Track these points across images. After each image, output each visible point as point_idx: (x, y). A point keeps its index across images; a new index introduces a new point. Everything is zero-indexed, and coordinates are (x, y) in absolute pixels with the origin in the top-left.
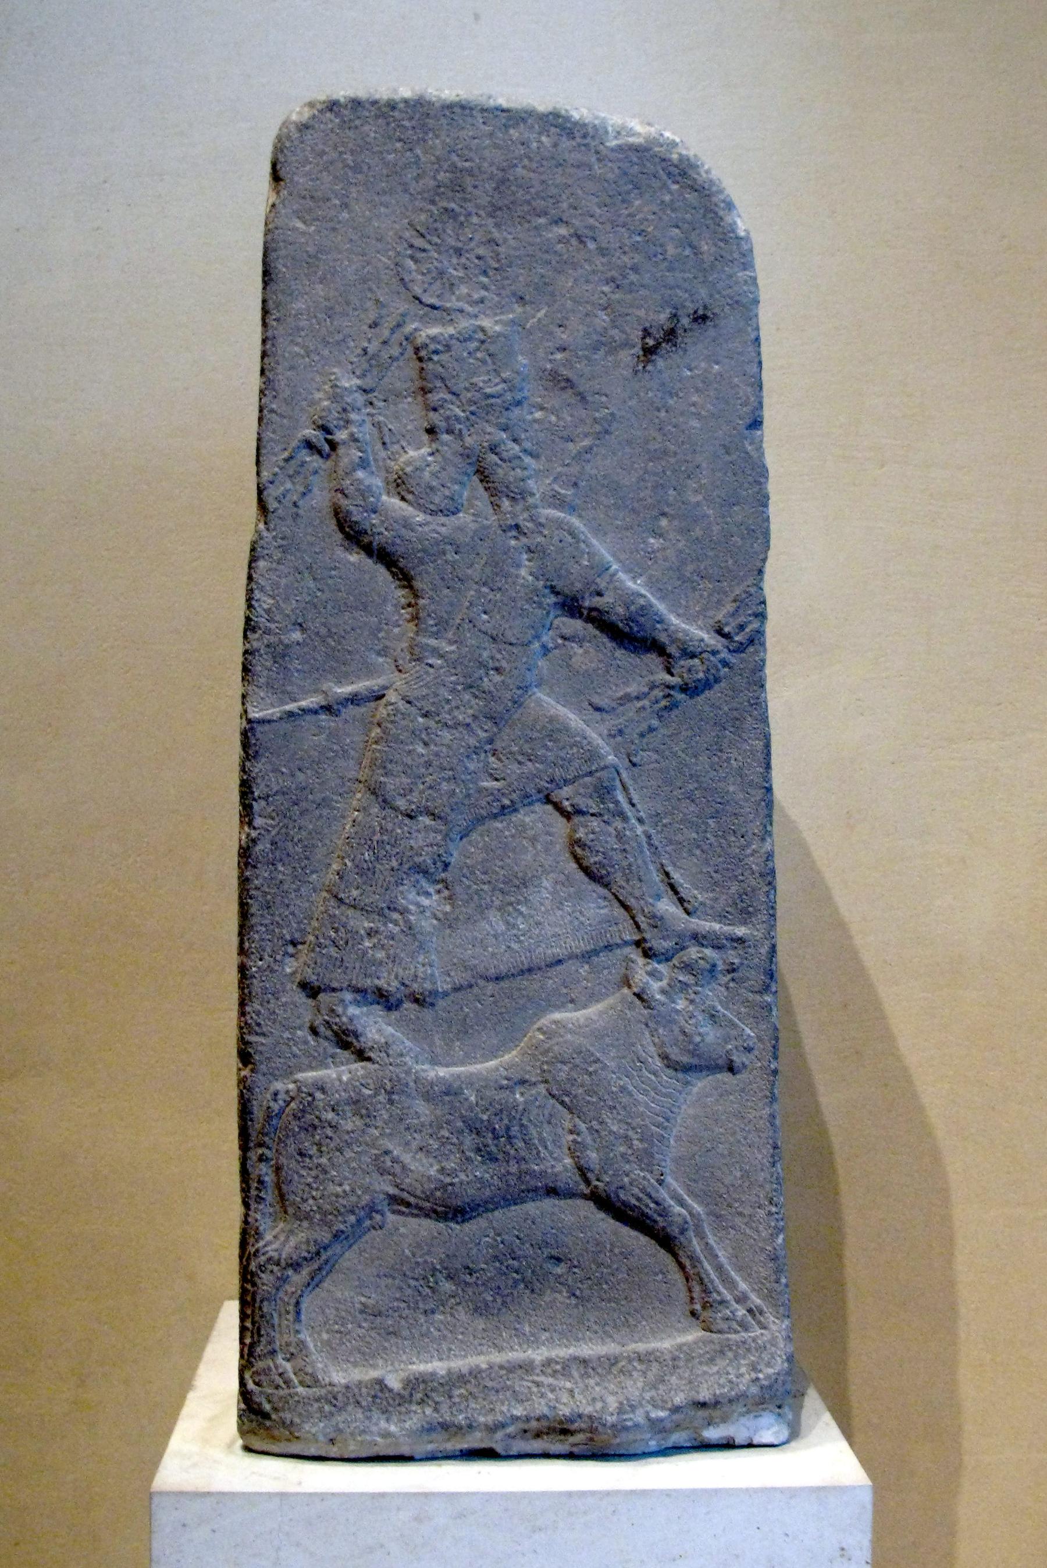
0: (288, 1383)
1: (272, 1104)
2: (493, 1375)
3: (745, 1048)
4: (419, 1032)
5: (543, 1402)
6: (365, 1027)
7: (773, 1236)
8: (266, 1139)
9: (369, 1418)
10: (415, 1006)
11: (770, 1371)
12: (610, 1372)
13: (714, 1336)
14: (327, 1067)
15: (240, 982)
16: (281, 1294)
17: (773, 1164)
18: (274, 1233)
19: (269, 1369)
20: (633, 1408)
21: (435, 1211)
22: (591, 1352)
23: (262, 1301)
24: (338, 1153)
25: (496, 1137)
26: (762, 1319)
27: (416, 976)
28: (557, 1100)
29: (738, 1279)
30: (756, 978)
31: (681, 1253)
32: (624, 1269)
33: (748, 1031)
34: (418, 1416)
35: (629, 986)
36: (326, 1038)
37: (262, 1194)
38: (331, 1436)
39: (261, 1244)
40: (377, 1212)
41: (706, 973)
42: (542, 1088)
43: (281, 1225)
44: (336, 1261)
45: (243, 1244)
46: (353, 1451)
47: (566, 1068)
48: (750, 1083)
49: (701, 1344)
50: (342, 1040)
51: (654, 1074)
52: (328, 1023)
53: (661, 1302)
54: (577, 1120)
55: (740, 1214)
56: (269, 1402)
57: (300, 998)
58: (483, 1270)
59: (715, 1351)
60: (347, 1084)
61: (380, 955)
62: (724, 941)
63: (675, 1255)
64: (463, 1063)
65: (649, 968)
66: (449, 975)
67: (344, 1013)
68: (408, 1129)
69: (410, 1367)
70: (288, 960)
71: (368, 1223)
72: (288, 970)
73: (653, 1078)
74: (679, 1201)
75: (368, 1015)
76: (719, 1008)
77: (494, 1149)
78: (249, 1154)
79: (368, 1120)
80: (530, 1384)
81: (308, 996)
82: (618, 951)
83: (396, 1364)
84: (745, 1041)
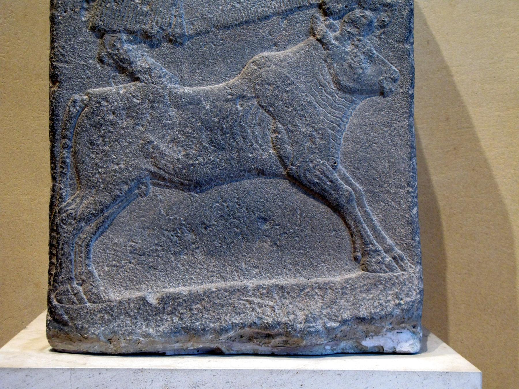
0: (80, 300)
1: (72, 109)
2: (220, 296)
3: (392, 79)
4: (173, 63)
5: (254, 314)
6: (136, 58)
7: (411, 208)
8: (68, 133)
9: (135, 324)
10: (168, 45)
11: (408, 299)
12: (299, 296)
13: (369, 273)
14: (110, 85)
15: (51, 27)
16: (77, 240)
17: (411, 159)
18: (72, 198)
19: (67, 290)
20: (315, 319)
21: (182, 184)
22: (287, 282)
23: (63, 244)
24: (117, 143)
25: (224, 134)
26: (402, 264)
27: (170, 23)
28: (265, 109)
29: (386, 237)
30: (400, 32)
31: (348, 217)
32: (309, 227)
33: (394, 68)
34: (169, 323)
35: (314, 35)
36: (109, 65)
37: (65, 171)
38: (109, 337)
39: (64, 204)
40: (143, 184)
41: (366, 27)
42: (255, 101)
43: (78, 192)
44: (115, 218)
45: (52, 205)
46: (123, 347)
47: (270, 88)
48: (395, 104)
49: (361, 279)
50: (120, 66)
51: (330, 94)
52: (110, 54)
53: (334, 250)
54: (278, 123)
55: (388, 192)
56: (67, 314)
57: (92, 38)
58: (214, 225)
59: (371, 284)
60: (123, 95)
61: (146, 8)
62: (378, 6)
63: (344, 219)
64: (201, 85)
65: (327, 23)
66: (193, 24)
67: (121, 48)
68: (164, 127)
69: (164, 290)
70: (83, 12)
71: (136, 191)
72: (84, 19)
73: (330, 97)
74: (346, 180)
75: (138, 50)
76: (375, 51)
77: (222, 141)
78: (56, 144)
79: (137, 120)
80: (244, 302)
81: (98, 37)
82: (307, 12)
83: (154, 288)
84: (392, 74)
